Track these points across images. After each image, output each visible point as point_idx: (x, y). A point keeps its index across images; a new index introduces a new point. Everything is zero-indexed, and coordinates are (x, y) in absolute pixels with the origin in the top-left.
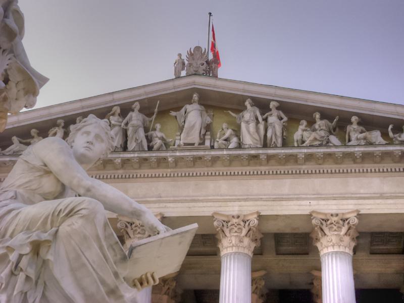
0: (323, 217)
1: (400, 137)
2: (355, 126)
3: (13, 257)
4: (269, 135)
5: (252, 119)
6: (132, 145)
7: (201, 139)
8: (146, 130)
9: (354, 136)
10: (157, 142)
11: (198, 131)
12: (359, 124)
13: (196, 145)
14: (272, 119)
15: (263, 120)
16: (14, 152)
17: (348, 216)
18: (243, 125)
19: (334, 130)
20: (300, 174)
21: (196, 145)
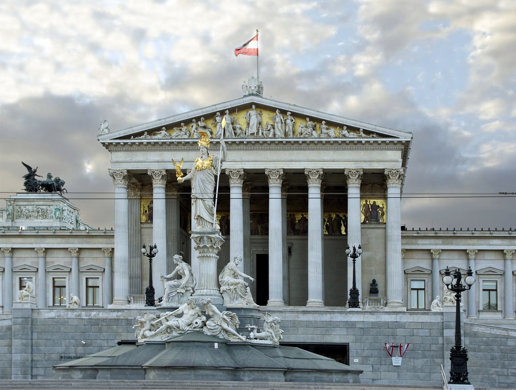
0: (309, 170)
1: (342, 132)
2: (324, 126)
3: (232, 290)
4: (287, 130)
5: (279, 121)
6: (227, 134)
7: (257, 130)
8: (232, 124)
9: (324, 131)
10: (238, 131)
11: (256, 126)
12: (326, 124)
13: (255, 134)
14: (288, 121)
15: (284, 120)
16: (176, 136)
17: (319, 170)
18: (276, 124)
19: (315, 126)
20: (300, 149)
21: (255, 134)
